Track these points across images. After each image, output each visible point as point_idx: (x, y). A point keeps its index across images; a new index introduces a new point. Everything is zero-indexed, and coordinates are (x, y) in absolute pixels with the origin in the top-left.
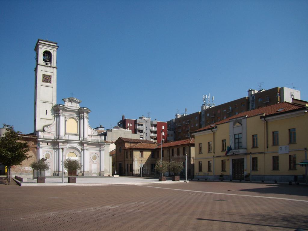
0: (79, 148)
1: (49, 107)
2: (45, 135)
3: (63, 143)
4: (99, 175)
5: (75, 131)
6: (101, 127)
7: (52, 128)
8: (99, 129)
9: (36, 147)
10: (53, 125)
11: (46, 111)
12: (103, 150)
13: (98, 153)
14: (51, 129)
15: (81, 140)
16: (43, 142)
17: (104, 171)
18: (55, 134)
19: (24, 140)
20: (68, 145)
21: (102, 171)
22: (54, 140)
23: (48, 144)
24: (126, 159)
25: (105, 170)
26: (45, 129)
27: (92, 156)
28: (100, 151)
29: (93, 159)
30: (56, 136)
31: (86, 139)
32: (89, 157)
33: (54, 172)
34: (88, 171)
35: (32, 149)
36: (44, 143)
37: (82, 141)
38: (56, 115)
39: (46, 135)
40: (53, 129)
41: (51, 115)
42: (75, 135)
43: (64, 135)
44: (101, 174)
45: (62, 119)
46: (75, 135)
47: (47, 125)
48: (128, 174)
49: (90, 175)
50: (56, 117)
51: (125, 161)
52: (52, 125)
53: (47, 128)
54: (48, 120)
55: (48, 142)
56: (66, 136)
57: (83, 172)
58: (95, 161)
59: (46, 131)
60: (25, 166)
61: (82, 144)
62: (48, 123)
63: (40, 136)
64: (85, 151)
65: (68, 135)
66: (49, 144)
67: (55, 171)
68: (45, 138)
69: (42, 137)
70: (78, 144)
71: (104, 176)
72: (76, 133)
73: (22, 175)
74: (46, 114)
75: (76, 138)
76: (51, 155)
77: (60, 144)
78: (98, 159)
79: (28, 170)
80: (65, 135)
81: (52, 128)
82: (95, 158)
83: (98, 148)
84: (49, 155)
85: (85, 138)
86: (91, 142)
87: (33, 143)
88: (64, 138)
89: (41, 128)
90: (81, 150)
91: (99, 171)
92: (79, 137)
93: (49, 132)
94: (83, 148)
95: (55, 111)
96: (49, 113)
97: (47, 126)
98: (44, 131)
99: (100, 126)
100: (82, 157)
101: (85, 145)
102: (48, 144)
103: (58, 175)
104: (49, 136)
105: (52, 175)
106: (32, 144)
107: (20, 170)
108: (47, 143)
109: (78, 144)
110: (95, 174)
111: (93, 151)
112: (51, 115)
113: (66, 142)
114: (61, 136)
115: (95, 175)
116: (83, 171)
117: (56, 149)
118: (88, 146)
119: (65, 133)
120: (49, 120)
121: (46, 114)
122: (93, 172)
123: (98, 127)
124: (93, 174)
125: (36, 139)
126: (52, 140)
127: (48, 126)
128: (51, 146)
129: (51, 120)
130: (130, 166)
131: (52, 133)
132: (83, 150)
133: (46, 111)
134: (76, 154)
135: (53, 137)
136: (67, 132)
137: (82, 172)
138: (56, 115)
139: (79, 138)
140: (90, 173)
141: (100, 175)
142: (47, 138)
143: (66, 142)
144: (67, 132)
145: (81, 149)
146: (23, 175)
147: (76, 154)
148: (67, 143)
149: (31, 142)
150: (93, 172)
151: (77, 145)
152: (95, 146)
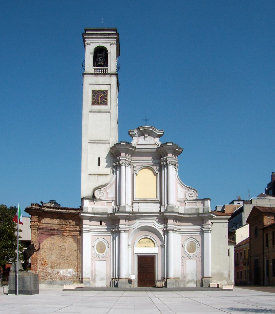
0: (160, 227)
1: (104, 151)
2: (95, 206)
3: (128, 218)
4: (199, 286)
5: (152, 194)
6: (239, 200)
7: (108, 191)
8: (236, 203)
9: (79, 231)
10: (111, 185)
11: (99, 158)
12: (209, 230)
13: (199, 238)
14: (107, 193)
15: (162, 211)
16: (91, 219)
17: (210, 276)
18: (114, 203)
19: (57, 218)
20: (138, 224)
21: (205, 276)
22: (111, 214)
23: (101, 224)
24: (266, 251)
25: (212, 275)
26: (97, 194)
27: (187, 243)
28: (202, 232)
29: (188, 250)
30: (115, 208)
31: (173, 207)
32: (180, 247)
33: (112, 279)
34: (179, 275)
35: (73, 234)
36: (93, 223)
37: (163, 213)
38: (114, 164)
39: (97, 207)
40: (110, 193)
41: (107, 167)
42: (152, 201)
43: (130, 203)
44: (204, 283)
45: (126, 171)
46: (152, 201)
47: (99, 186)
48: (269, 281)
49: (182, 286)
50: (116, 169)
51: (263, 253)
52: (108, 185)
53: (99, 192)
54: (101, 176)
55: (101, 219)
56: (134, 204)
57: (165, 279)
58: (193, 254)
59: (98, 197)
60: (60, 268)
61: (163, 219)
62: (102, 181)
63: (86, 207)
64: (171, 234)
65: (139, 203)
66: (103, 224)
67: (114, 277)
68: (95, 211)
69: (90, 210)
70: (157, 220)
71: (209, 287)
72: (156, 197)
73: (53, 284)
74: (99, 165)
75: (154, 208)
76: (106, 245)
77: (122, 222)
78: (198, 250)
79: (64, 275)
80: (133, 204)
81: (108, 191)
82: (192, 249)
83: (198, 228)
84: (104, 245)
85: (170, 206)
86: (184, 214)
87: (74, 223)
88: (128, 209)
89: (89, 193)
90: (162, 233)
91: (200, 277)
92: (159, 205)
93: (102, 199)
94: (167, 227)
95: (114, 158)
96: (103, 163)
97: (99, 188)
98: (93, 198)
99: (237, 199)
100: (165, 247)
101: (170, 221)
102: (101, 224)
103: (116, 285)
104: (104, 207)
105: (109, 284)
106: (72, 224)
107: (50, 274)
108: (99, 223)
109: (157, 220)
110: (193, 283)
111: (189, 234)
112: (107, 167)
113: (132, 217)
114: (122, 205)
115: (193, 285)
116: (167, 277)
117: (116, 232)
118: (178, 223)
119: (133, 200)
120: (104, 177)
121: (99, 165)
122: (189, 278)
123: (234, 201)
124: (188, 282)
125: (79, 213)
126: (108, 214)
127: (102, 189)
128: (106, 227)
129: (107, 175)
130: (271, 264)
131: (108, 202)
132: (166, 232)
133: (99, 158)
134: (149, 239)
135: (109, 209)
136: (136, 197)
137: (165, 280)
138: (114, 164)
139: (160, 207)
140: (182, 281)
141: (202, 285)
142: (100, 211)
143: (132, 217)
144: (136, 197)
145: (164, 231)
146: (56, 284)
147: (149, 239)
148: (135, 218)
149: (71, 221)
150: (189, 278)
151: (154, 221)
152: (191, 224)
